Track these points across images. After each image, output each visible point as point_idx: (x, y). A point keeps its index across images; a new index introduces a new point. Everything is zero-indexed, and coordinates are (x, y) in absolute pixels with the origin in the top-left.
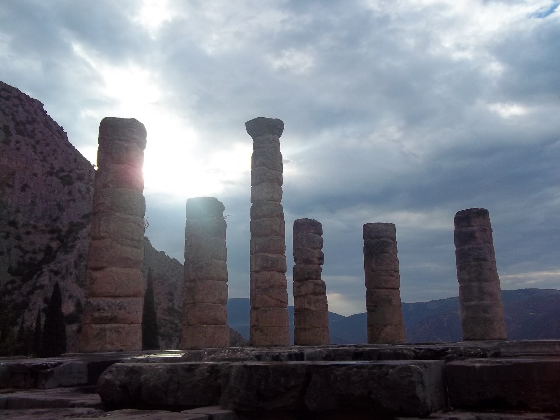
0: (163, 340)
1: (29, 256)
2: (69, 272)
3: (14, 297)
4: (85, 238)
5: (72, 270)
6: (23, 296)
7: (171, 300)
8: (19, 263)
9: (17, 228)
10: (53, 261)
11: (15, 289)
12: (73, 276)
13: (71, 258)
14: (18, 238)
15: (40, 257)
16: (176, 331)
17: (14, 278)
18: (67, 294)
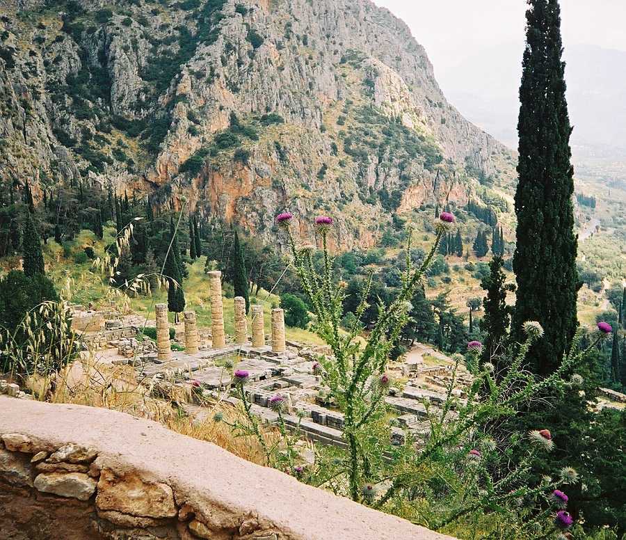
0: (354, 161)
1: (162, 48)
2: (215, 73)
3: (151, 110)
4: (232, 17)
5: (222, 71)
6: (162, 109)
7: (370, 94)
8: (149, 60)
9: (140, 6)
10: (193, 55)
11: (148, 100)
12: (222, 78)
13: (217, 49)
14: (143, 22)
15: (175, 48)
16: (375, 147)
17: (146, 82)
18: (218, 106)
